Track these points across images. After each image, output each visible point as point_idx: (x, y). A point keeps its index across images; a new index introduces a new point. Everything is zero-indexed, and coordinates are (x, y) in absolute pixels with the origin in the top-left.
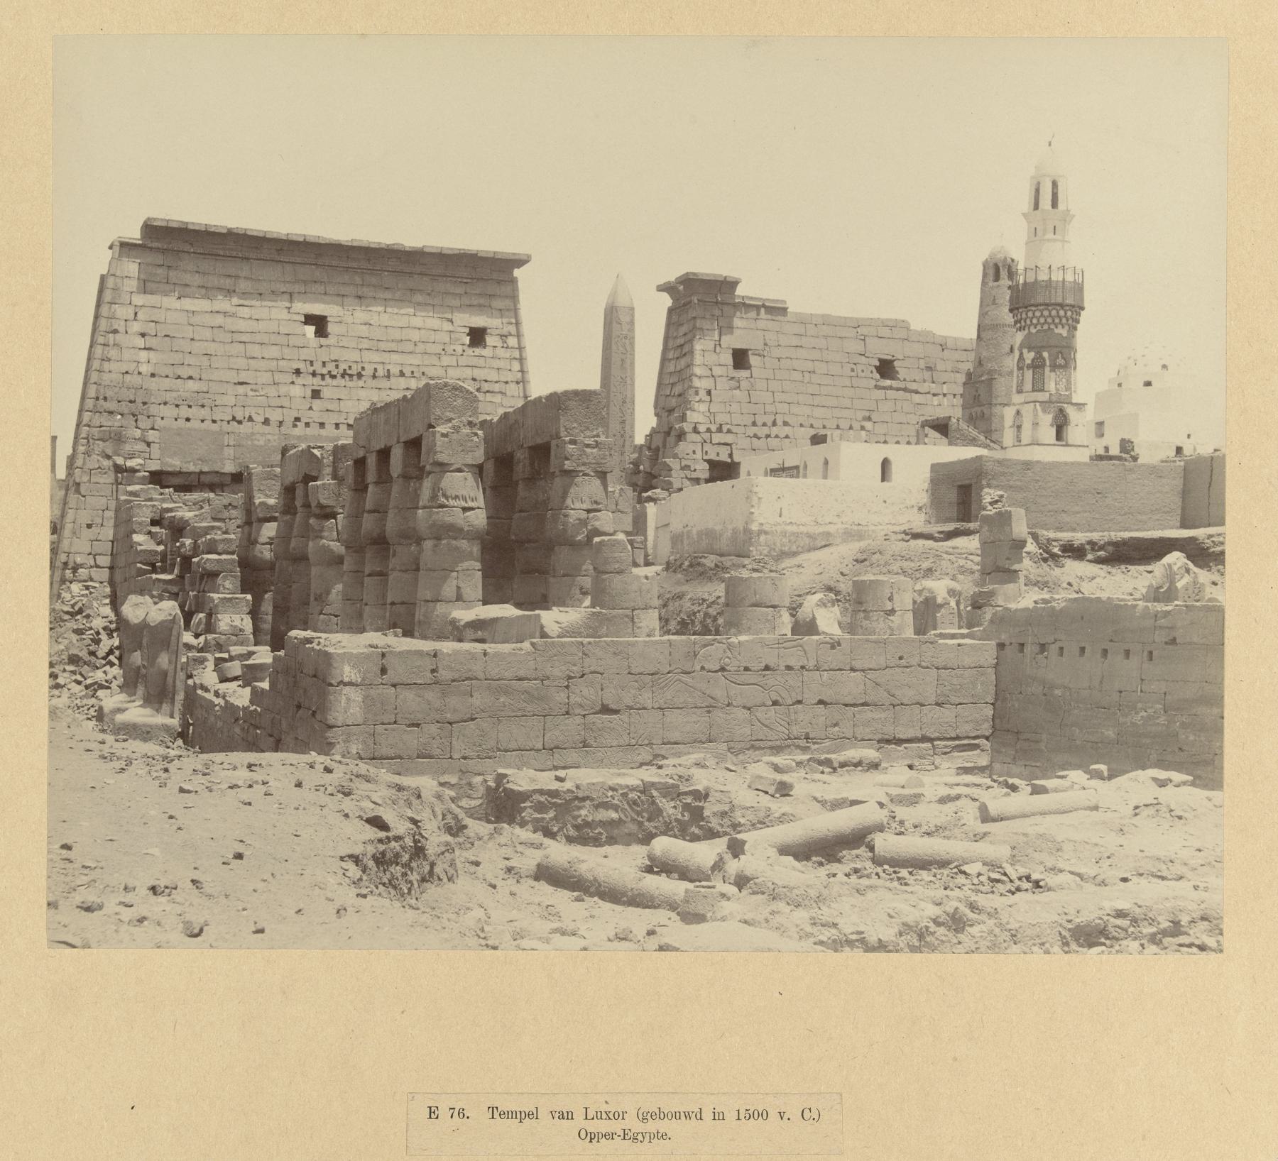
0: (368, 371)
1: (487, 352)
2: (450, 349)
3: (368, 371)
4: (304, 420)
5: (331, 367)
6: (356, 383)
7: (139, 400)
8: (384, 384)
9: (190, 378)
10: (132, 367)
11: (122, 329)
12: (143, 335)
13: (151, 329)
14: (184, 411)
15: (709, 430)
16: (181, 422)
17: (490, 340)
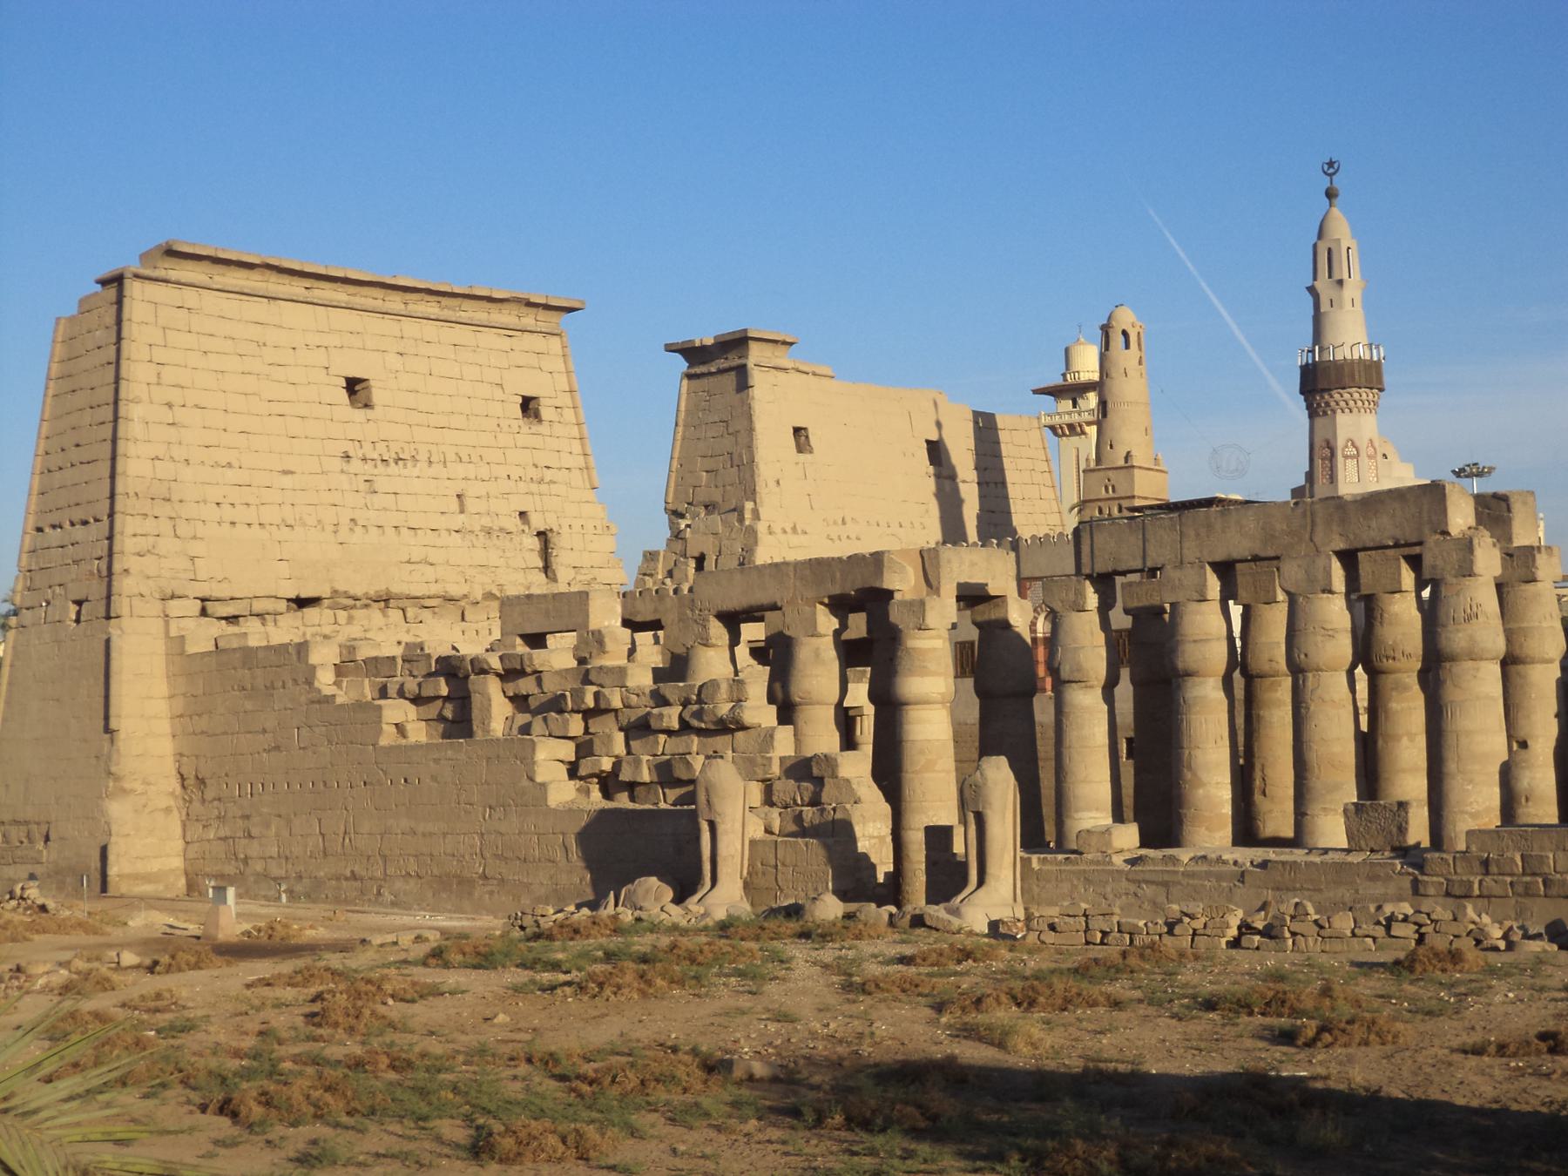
0: (423, 456)
1: (543, 428)
2: (504, 423)
3: (423, 456)
4: (361, 522)
5: (381, 447)
6: (411, 470)
7: (175, 498)
8: (437, 469)
9: (229, 465)
10: (160, 450)
11: (145, 397)
12: (170, 405)
13: (175, 396)
14: (228, 513)
15: (785, 532)
16: (226, 526)
17: (546, 413)
